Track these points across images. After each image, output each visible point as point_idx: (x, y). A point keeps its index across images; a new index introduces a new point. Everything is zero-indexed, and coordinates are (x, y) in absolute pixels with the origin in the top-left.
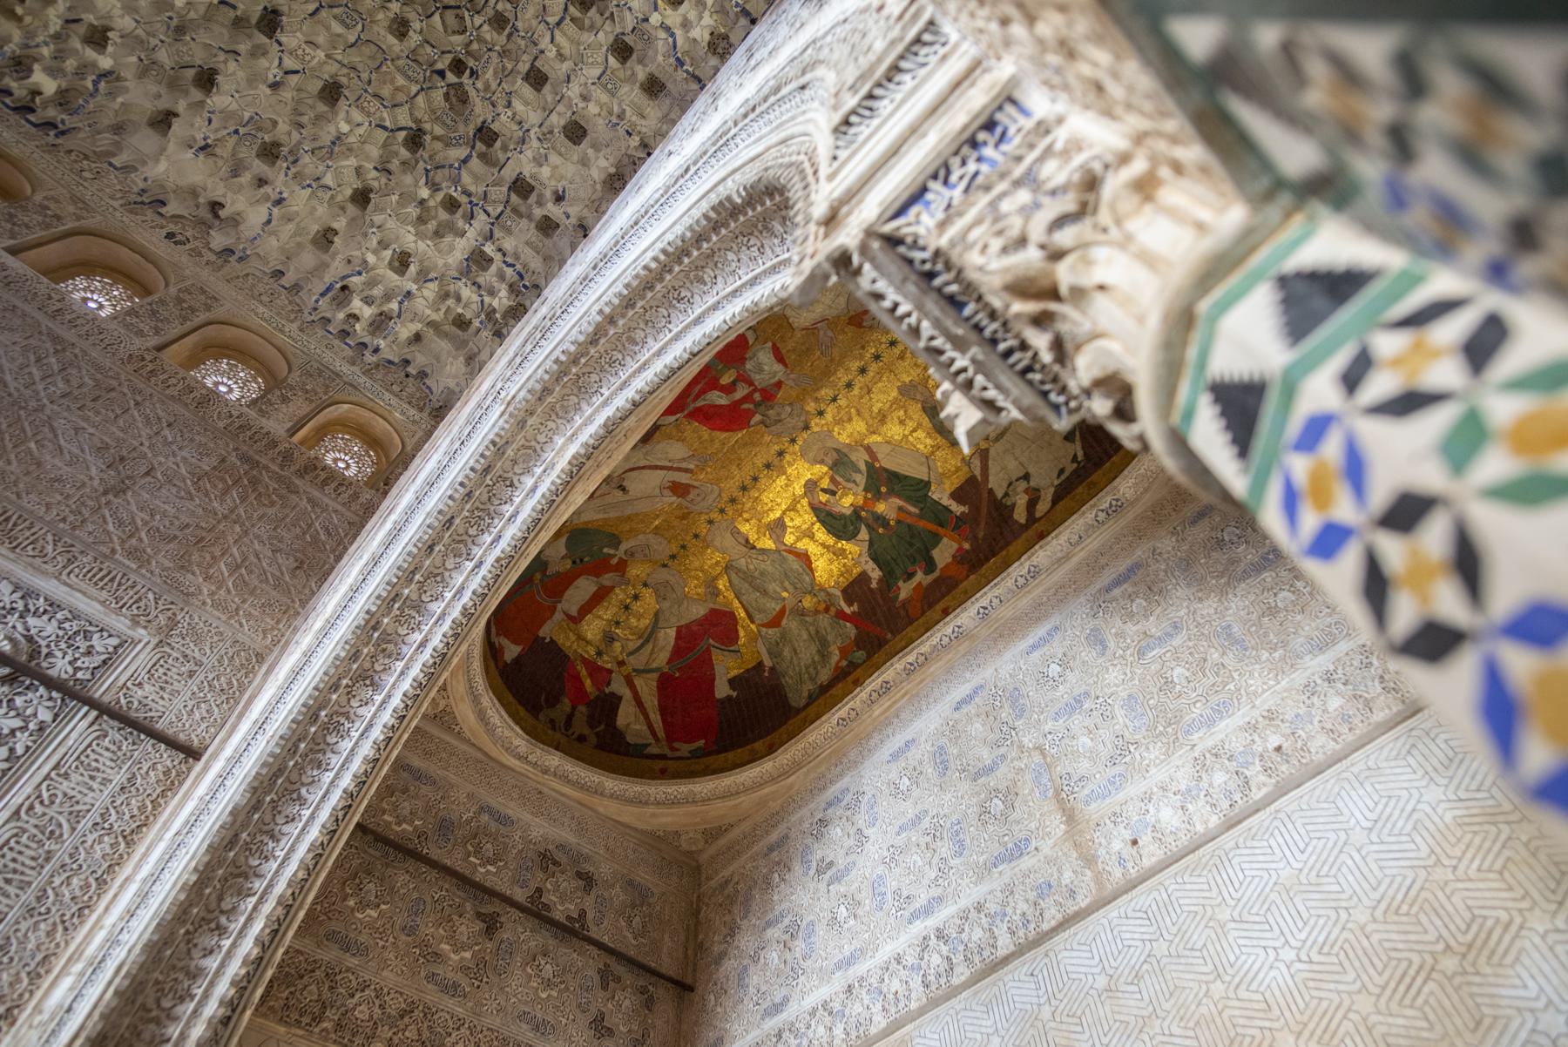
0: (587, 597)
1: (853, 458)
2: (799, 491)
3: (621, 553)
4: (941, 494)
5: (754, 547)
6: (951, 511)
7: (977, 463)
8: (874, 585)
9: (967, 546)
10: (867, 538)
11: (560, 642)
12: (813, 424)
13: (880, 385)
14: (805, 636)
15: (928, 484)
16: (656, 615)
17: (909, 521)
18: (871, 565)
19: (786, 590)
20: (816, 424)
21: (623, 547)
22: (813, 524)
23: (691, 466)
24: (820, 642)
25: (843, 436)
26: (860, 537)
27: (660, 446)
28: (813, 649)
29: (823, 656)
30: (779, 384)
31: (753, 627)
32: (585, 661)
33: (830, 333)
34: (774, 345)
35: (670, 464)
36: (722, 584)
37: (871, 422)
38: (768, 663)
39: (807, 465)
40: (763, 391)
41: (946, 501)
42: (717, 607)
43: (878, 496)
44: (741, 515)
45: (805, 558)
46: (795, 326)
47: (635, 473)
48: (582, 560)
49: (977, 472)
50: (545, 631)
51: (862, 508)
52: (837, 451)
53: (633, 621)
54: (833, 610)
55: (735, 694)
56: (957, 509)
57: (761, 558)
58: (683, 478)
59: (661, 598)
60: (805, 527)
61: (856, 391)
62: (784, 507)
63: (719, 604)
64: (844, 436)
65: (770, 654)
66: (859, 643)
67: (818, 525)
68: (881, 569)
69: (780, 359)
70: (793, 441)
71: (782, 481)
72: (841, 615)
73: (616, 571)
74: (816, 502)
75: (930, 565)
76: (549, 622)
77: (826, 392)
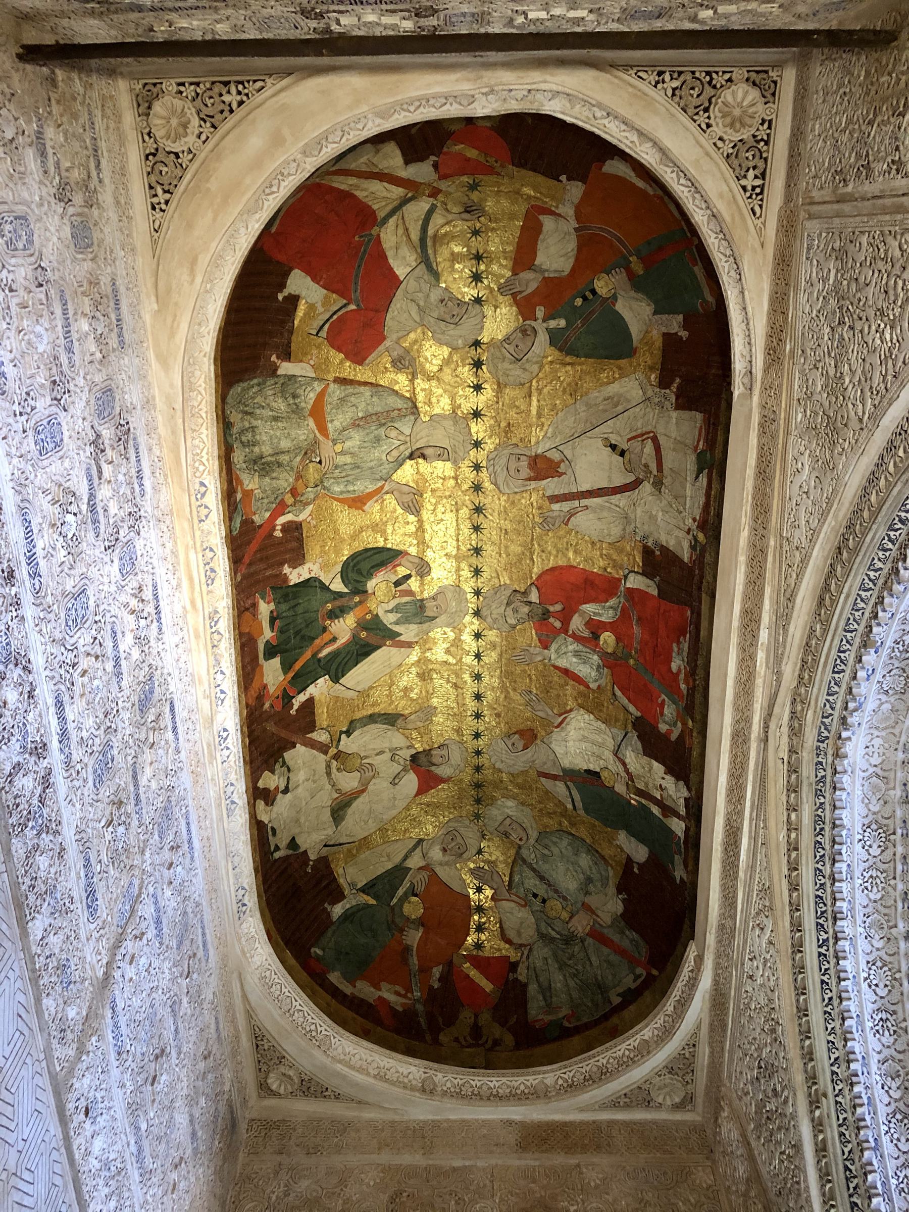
0: (541, 246)
1: (413, 627)
2: (429, 555)
3: (539, 326)
4: (320, 688)
5: (411, 457)
6: (299, 693)
7: (321, 736)
8: (286, 569)
9: (267, 705)
10: (332, 587)
11: (540, 179)
12: (475, 620)
13: (453, 697)
14: (285, 444)
15: (336, 679)
16: (436, 275)
17: (318, 642)
18: (306, 576)
19: (342, 453)
20: (472, 623)
21: (543, 338)
22: (386, 539)
23: (556, 507)
24: (268, 464)
25: (441, 635)
26: (338, 579)
27: (616, 531)
28: (266, 449)
29: (255, 462)
30: (546, 647)
31: (331, 377)
32: (490, 170)
33: (540, 714)
34: (588, 687)
35: (584, 502)
36: (402, 381)
37: (430, 667)
38: (286, 368)
39: (446, 582)
40: (556, 632)
41: (311, 690)
42: (381, 348)
43: (363, 625)
44: (456, 478)
45: (358, 502)
46: (582, 711)
47: (618, 482)
48: (585, 298)
49: (314, 735)
50: (575, 190)
51: (360, 602)
52: (435, 618)
53: (457, 249)
54: (289, 500)
55: (280, 297)
56: (300, 700)
57: (395, 454)
58: (552, 486)
59: (449, 299)
60: (389, 529)
61: (467, 677)
62: (427, 526)
63: (382, 357)
64: (438, 636)
65: (293, 378)
66: (247, 523)
67: (381, 544)
68: (296, 585)
69: (566, 672)
70: (477, 593)
71: (452, 549)
72: (282, 508)
73: (528, 298)
74: (404, 561)
75: (271, 652)
76: (576, 201)
77: (490, 657)
